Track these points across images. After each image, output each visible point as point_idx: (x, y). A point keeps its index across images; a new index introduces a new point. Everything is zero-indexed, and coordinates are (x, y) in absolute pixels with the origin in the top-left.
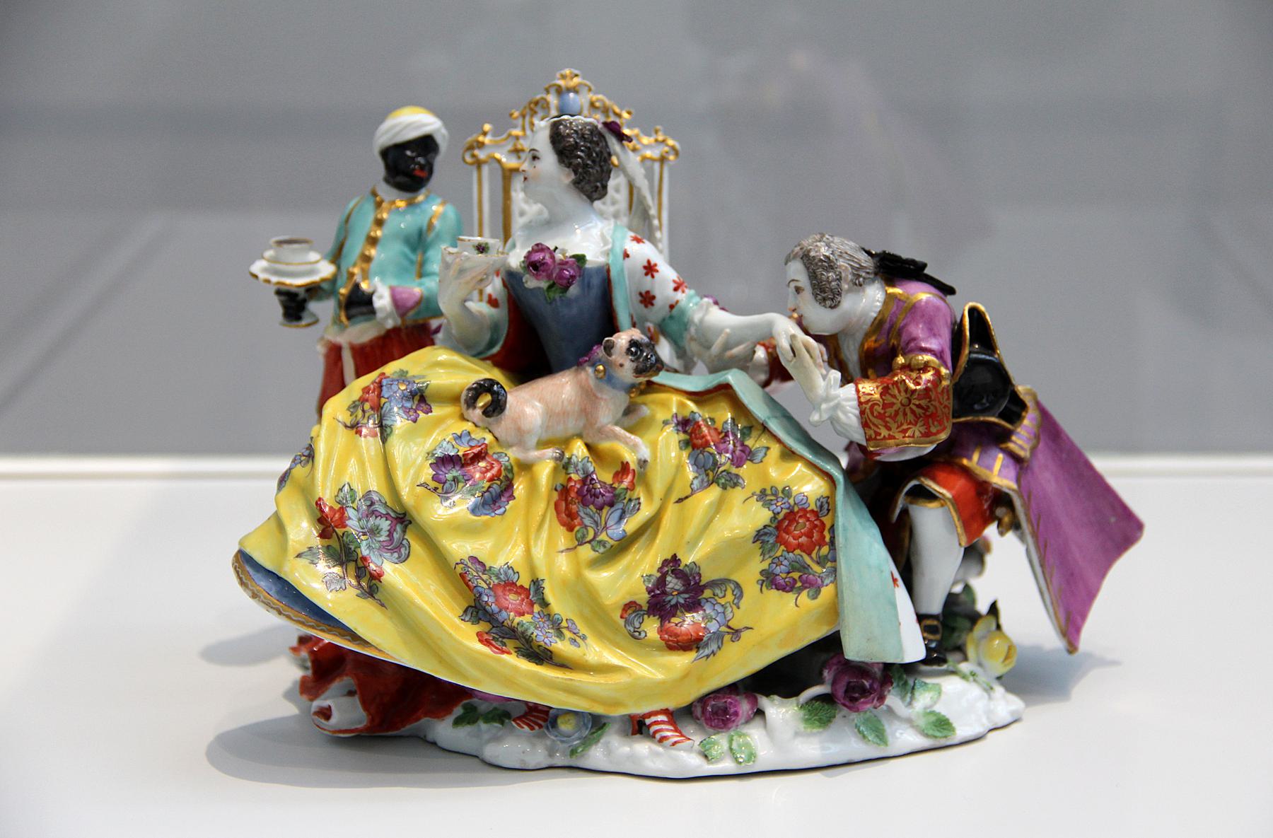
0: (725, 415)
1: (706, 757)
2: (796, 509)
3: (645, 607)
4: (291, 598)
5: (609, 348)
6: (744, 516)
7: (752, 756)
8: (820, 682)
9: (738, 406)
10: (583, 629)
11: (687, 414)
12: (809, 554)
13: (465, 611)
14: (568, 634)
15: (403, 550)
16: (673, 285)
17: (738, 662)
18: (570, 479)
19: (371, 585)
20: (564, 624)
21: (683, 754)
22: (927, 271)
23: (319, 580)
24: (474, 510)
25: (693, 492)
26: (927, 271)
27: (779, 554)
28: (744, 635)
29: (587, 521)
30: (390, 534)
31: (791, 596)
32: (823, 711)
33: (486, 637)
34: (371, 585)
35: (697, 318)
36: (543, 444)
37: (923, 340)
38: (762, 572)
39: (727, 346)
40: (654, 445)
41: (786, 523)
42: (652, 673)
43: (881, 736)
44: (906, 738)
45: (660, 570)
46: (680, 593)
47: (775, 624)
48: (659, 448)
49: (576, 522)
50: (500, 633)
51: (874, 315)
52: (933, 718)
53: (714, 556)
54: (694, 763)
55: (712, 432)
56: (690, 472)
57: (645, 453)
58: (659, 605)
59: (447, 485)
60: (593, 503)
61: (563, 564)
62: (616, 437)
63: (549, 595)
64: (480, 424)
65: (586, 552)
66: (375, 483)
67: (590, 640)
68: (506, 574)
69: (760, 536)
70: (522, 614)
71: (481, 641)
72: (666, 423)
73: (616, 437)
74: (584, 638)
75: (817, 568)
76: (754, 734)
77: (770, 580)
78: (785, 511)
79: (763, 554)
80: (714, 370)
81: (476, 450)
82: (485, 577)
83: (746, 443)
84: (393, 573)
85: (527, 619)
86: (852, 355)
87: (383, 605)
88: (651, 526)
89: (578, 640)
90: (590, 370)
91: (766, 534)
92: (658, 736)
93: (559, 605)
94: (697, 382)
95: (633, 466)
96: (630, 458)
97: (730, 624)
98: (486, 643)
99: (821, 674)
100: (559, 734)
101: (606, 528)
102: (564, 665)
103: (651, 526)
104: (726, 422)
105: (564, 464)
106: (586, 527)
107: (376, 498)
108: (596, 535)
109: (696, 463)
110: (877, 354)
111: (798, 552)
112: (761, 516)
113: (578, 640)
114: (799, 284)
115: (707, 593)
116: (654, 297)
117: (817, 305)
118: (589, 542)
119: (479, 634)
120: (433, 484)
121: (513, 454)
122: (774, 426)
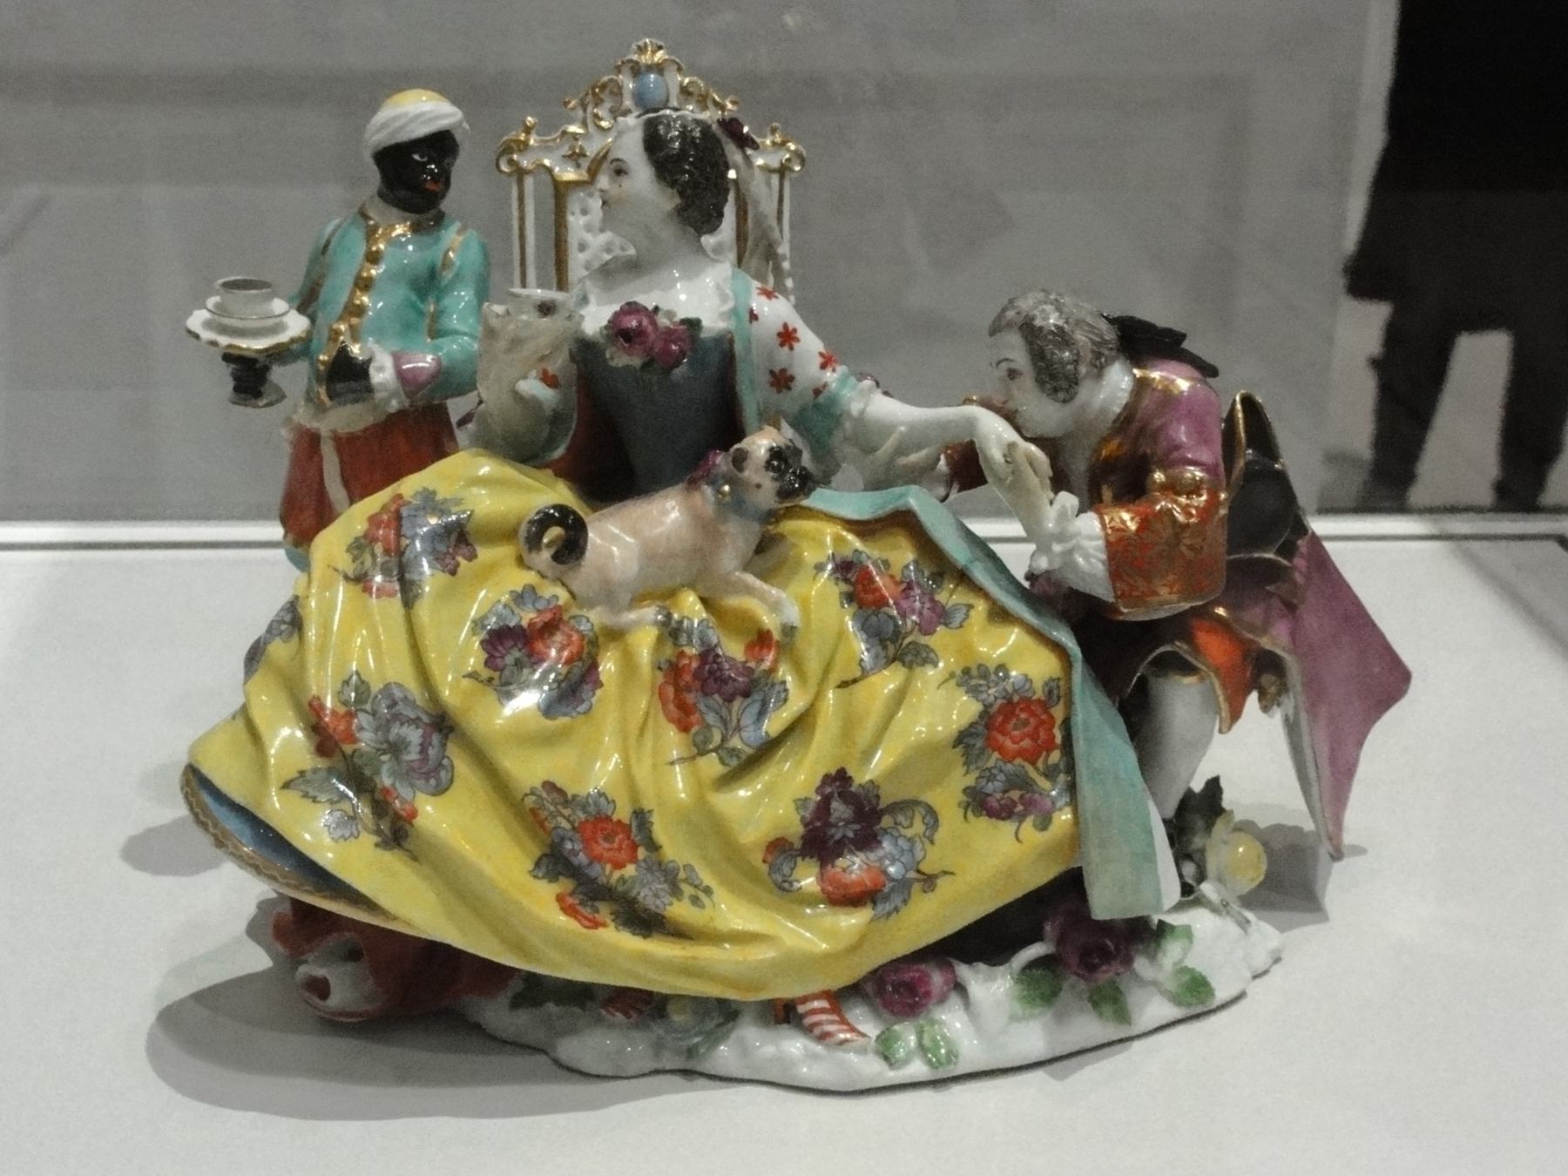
0: (902, 555)
1: (886, 1058)
2: (1016, 698)
3: (798, 844)
4: (273, 846)
5: (740, 460)
6: (937, 708)
7: (952, 1055)
8: (1035, 937)
9: (927, 546)
10: (707, 878)
11: (847, 553)
12: (1033, 763)
13: (537, 864)
14: (687, 890)
15: (443, 774)
16: (819, 360)
17: (928, 919)
18: (682, 654)
19: (397, 832)
20: (682, 875)
21: (852, 1056)
22: (1186, 345)
23: (317, 830)
24: (548, 710)
25: (865, 674)
26: (1186, 345)
27: (991, 763)
28: (942, 882)
29: (711, 718)
30: (423, 749)
31: (1008, 827)
32: (1043, 984)
33: (570, 900)
34: (397, 832)
35: (855, 408)
36: (638, 600)
37: (1189, 450)
38: (966, 790)
39: (901, 450)
40: (804, 604)
41: (1000, 719)
42: (812, 937)
43: (1123, 1016)
44: (1153, 1009)
45: (819, 790)
46: (848, 823)
47: (989, 862)
48: (806, 601)
49: (694, 718)
50: (590, 895)
51: (1118, 410)
52: (1186, 978)
53: (895, 772)
54: (872, 1069)
55: (888, 580)
56: (860, 647)
57: (793, 614)
58: (818, 842)
59: (507, 672)
60: (719, 691)
61: (679, 783)
62: (749, 590)
63: (660, 833)
64: (549, 574)
65: (711, 766)
66: (400, 672)
67: (720, 893)
68: (596, 804)
69: (963, 739)
70: (619, 865)
71: (563, 909)
72: (820, 568)
73: (749, 590)
74: (708, 891)
75: (1043, 783)
76: (951, 1020)
77: (978, 803)
78: (1000, 702)
79: (967, 763)
80: (875, 485)
81: (548, 617)
82: (567, 812)
83: (937, 598)
84: (433, 815)
85: (630, 870)
86: (1079, 467)
87: (415, 859)
88: (801, 725)
89: (702, 896)
90: (708, 490)
91: (971, 735)
92: (817, 1031)
93: (674, 847)
94: (861, 505)
95: (776, 636)
96: (769, 621)
97: (923, 867)
98: (568, 910)
99: (1042, 929)
100: (676, 1031)
101: (738, 729)
102: (680, 933)
103: (801, 725)
104: (907, 567)
105: (672, 631)
106: (708, 727)
107: (398, 694)
108: (724, 740)
109: (865, 627)
110: (1116, 467)
111: (1018, 761)
112: (963, 709)
113: (702, 896)
114: (1013, 366)
115: (886, 821)
116: (792, 378)
117: (1044, 398)
118: (715, 750)
119: (560, 898)
120: (485, 673)
121: (596, 617)
122: (980, 574)
